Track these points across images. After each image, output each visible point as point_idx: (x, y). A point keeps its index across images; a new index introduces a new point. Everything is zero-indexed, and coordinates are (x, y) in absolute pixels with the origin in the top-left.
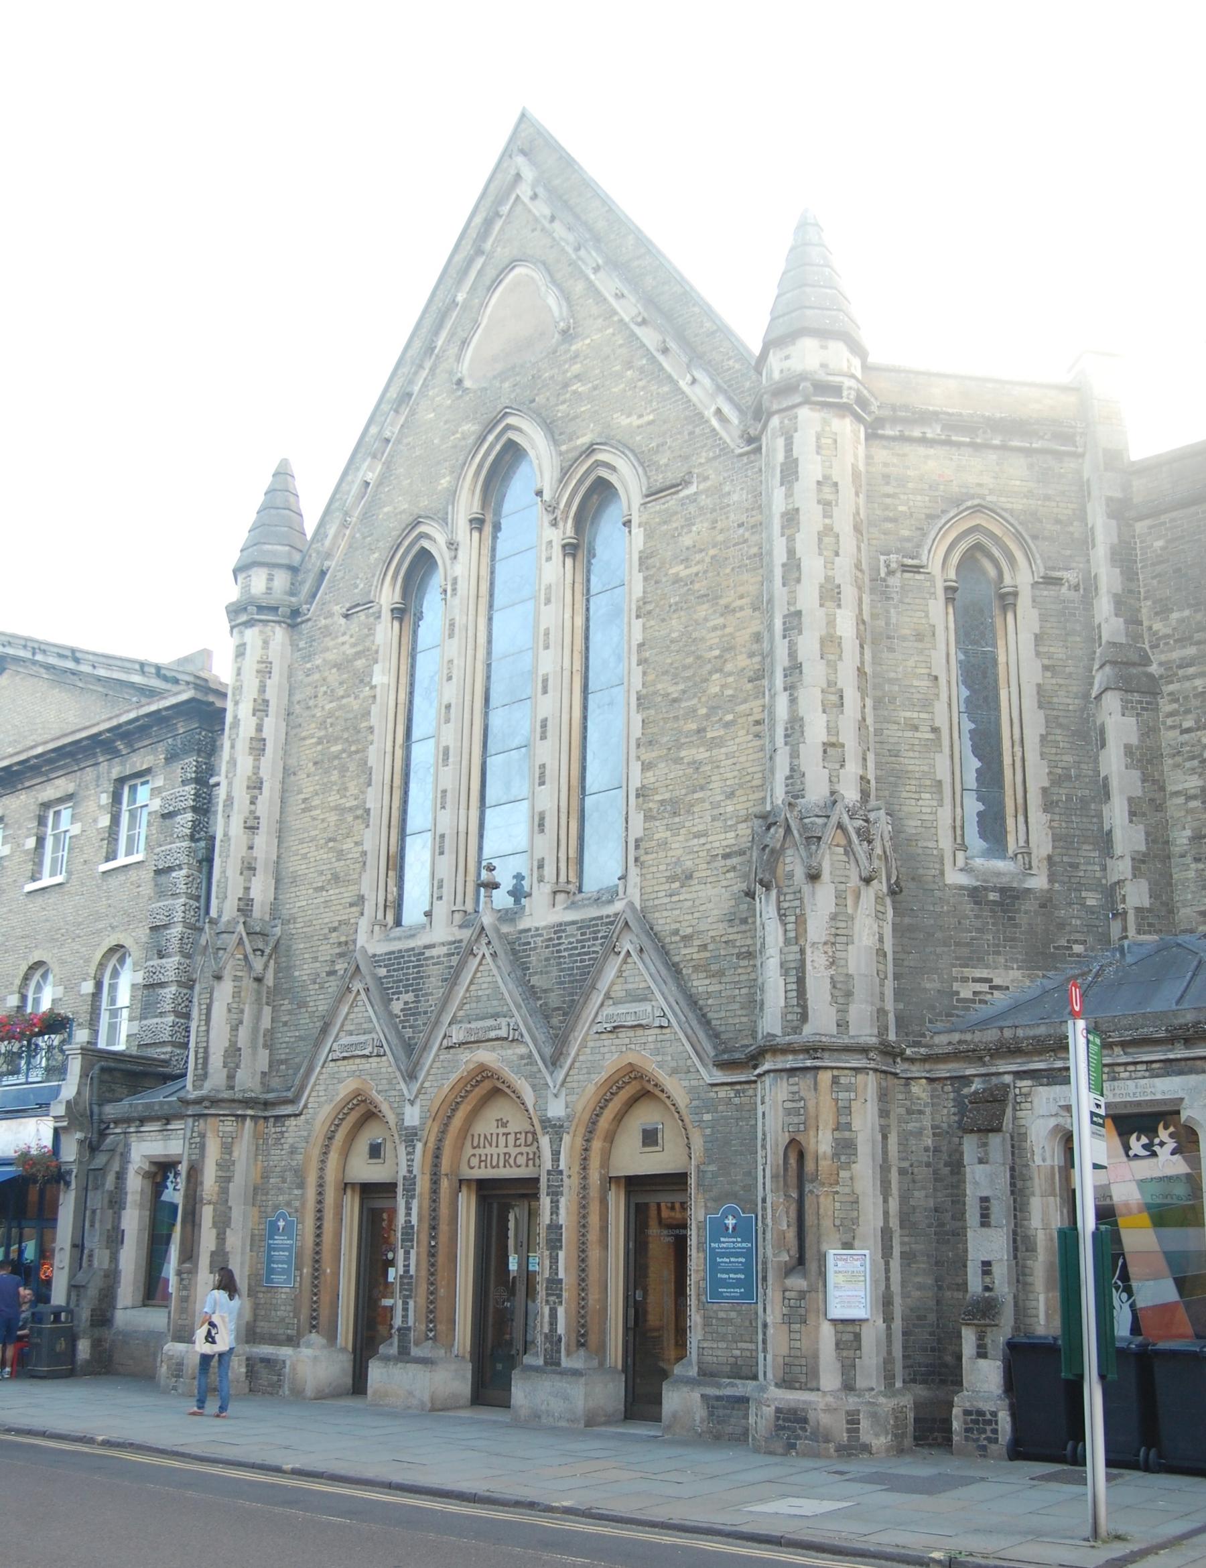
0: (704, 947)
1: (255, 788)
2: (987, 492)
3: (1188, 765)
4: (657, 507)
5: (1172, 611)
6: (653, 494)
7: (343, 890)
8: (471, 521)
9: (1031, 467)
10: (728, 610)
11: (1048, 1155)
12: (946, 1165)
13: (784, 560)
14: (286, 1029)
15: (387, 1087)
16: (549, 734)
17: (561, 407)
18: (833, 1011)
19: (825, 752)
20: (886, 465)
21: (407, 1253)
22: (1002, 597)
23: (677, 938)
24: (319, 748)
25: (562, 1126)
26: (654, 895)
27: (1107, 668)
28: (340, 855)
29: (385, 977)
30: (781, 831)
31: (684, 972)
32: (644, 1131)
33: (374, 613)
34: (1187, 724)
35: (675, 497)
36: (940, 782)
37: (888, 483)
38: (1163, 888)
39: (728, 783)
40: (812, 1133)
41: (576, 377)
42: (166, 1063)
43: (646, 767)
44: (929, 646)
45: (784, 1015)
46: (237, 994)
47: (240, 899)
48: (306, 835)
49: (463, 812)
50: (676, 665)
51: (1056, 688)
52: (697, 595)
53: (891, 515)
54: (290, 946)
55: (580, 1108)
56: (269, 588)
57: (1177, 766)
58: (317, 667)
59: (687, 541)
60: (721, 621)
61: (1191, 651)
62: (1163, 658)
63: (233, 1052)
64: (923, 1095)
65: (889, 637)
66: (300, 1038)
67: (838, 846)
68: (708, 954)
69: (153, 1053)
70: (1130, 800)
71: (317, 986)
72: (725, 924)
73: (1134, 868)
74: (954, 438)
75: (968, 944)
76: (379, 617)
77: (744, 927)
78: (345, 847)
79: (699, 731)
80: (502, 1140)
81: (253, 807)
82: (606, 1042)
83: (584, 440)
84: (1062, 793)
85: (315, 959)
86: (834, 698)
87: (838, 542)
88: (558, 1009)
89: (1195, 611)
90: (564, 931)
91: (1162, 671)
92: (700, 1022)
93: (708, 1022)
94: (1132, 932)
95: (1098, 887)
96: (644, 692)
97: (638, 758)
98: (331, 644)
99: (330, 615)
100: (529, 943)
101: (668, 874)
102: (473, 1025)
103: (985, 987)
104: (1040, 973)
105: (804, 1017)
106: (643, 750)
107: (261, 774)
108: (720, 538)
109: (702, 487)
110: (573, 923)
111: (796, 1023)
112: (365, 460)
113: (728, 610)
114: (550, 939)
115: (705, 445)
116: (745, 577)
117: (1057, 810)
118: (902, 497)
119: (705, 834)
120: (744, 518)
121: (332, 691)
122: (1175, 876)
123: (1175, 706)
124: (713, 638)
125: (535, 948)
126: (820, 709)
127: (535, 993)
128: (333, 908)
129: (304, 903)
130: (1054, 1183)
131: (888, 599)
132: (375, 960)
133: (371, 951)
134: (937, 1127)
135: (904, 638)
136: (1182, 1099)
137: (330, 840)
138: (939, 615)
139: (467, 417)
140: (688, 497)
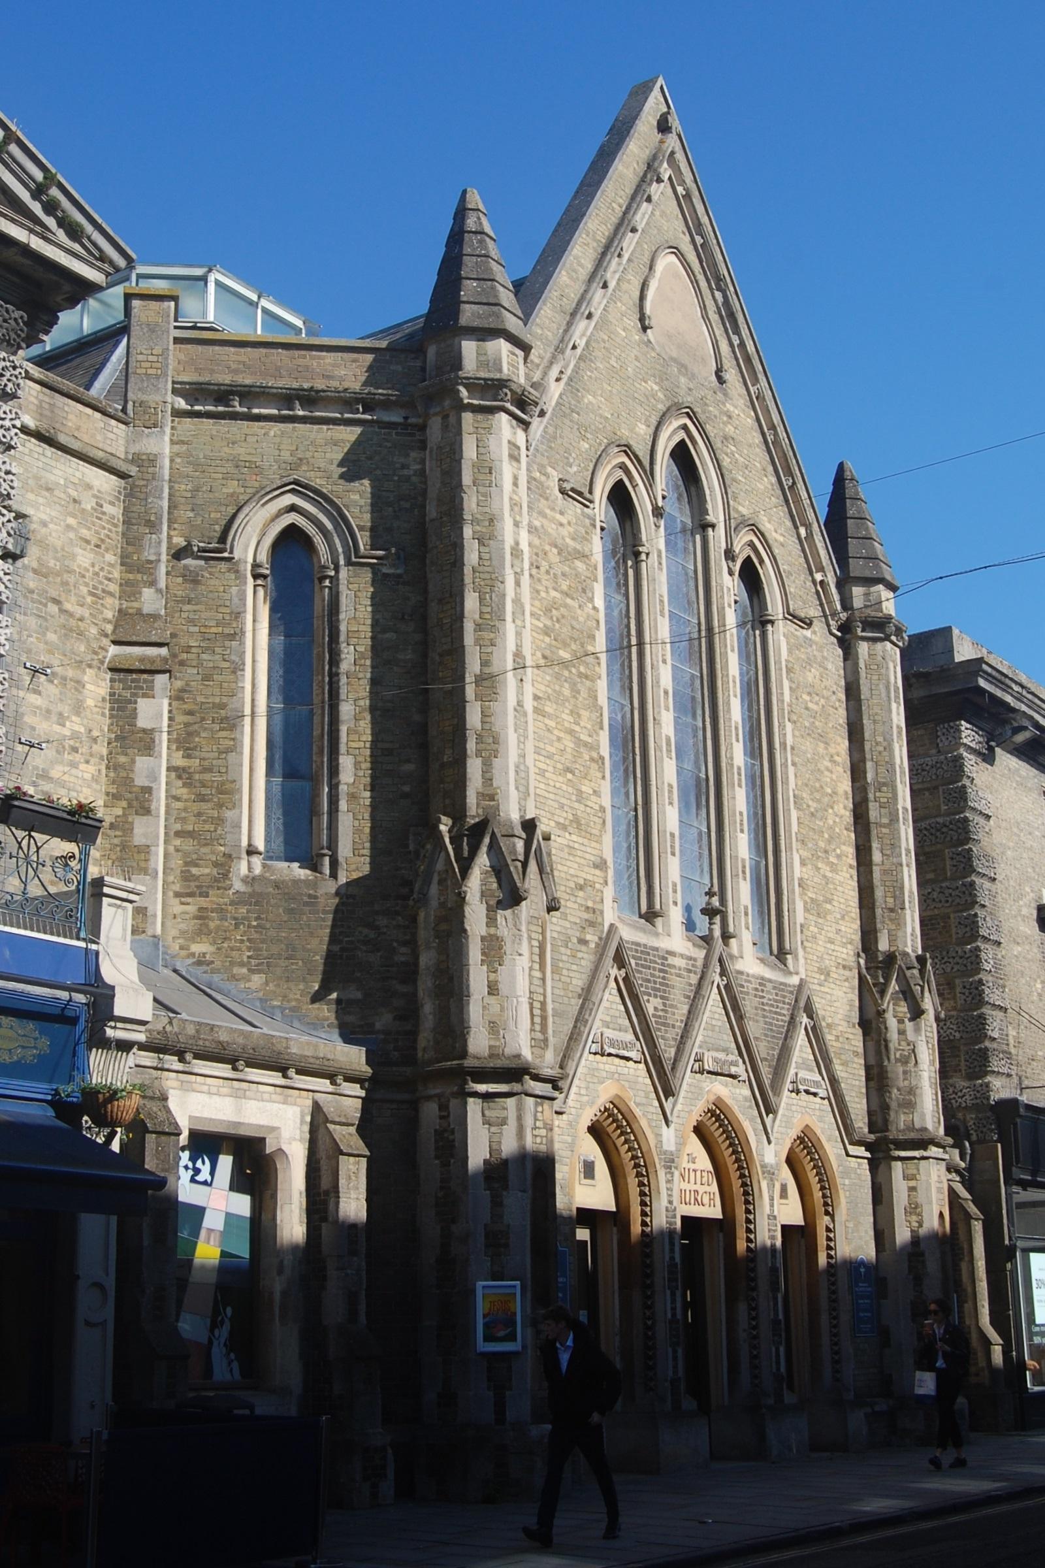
24: (547, 639)
110: (770, 981)
128: (578, 859)
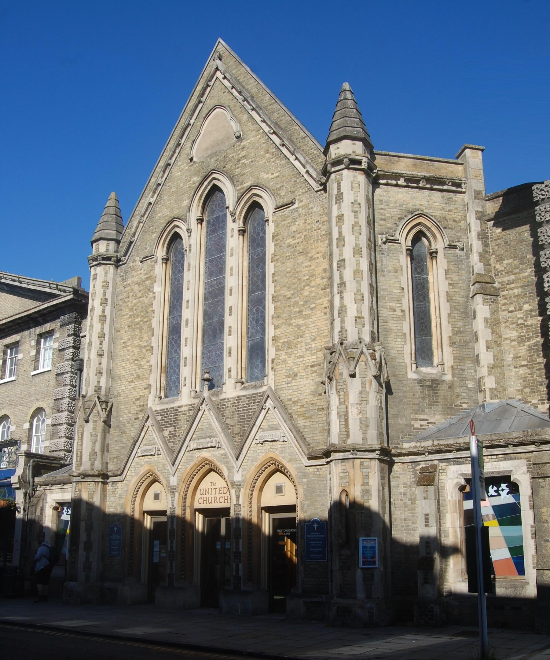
0: (303, 406)
1: (101, 337)
2: (424, 208)
3: (511, 326)
4: (280, 213)
5: (504, 260)
6: (278, 208)
7: (141, 382)
8: (197, 220)
9: (443, 197)
10: (312, 259)
11: (454, 495)
12: (409, 500)
13: (338, 237)
14: (116, 443)
15: (162, 468)
16: (233, 313)
17: (237, 170)
18: (361, 433)
19: (356, 320)
20: (381, 196)
21: (172, 541)
22: (431, 254)
23: (291, 402)
24: (130, 319)
25: (240, 485)
26: (280, 384)
27: (476, 285)
28: (140, 366)
29: (161, 420)
30: (337, 355)
31: (294, 417)
32: (276, 486)
33: (154, 260)
34: (511, 309)
35: (288, 209)
36: (405, 334)
37: (382, 204)
38: (501, 380)
39: (313, 334)
40: (352, 487)
41: (243, 157)
42: (61, 459)
43: (276, 327)
44: (400, 274)
45: (339, 435)
46: (95, 428)
47: (95, 386)
48: (124, 358)
49: (194, 347)
50: (289, 283)
51: (455, 293)
52: (298, 252)
53: (383, 217)
54: (118, 407)
55: (248, 476)
56: (107, 250)
57: (507, 327)
58: (129, 284)
59: (294, 228)
60: (309, 263)
61: (513, 277)
62: (500, 280)
63: (93, 453)
64: (399, 470)
65: (382, 271)
66: (123, 447)
67: (362, 361)
68: (304, 409)
69: (55, 454)
70: (487, 341)
71: (130, 425)
72: (312, 396)
73: (489, 371)
74: (410, 184)
75: (418, 404)
76: (156, 262)
77: (320, 397)
78: (142, 363)
79: (299, 312)
80: (213, 491)
81: (101, 346)
82: (260, 448)
83: (248, 184)
84: (457, 339)
85: (129, 413)
86: (360, 297)
87: (361, 229)
88: (238, 433)
89: (514, 260)
90: (240, 399)
91: (500, 286)
92: (301, 439)
93: (305, 439)
94: (488, 399)
95: (473, 379)
96: (275, 294)
97: (273, 323)
98: (135, 274)
99: (135, 261)
100: (225, 405)
101: (286, 374)
102: (201, 441)
103: (425, 423)
104: (449, 417)
105: (348, 436)
106: (275, 320)
107: (104, 332)
108: (309, 227)
109: (300, 205)
110: (245, 396)
111: (344, 439)
112: (149, 193)
113: (312, 259)
114: (234, 403)
115: (301, 187)
116: (320, 244)
117: (455, 346)
118: (388, 210)
119: (302, 357)
120: (318, 219)
121: (136, 295)
122: (506, 374)
123: (506, 301)
124: (306, 271)
125: (228, 407)
126: (354, 302)
127: (228, 427)
128: (137, 390)
129: (124, 388)
130: (456, 507)
131: (382, 254)
132: (157, 413)
133: (154, 409)
134: (406, 484)
135: (389, 271)
136: (512, 471)
137: (135, 360)
138: (405, 262)
139: (195, 174)
140: (294, 209)
